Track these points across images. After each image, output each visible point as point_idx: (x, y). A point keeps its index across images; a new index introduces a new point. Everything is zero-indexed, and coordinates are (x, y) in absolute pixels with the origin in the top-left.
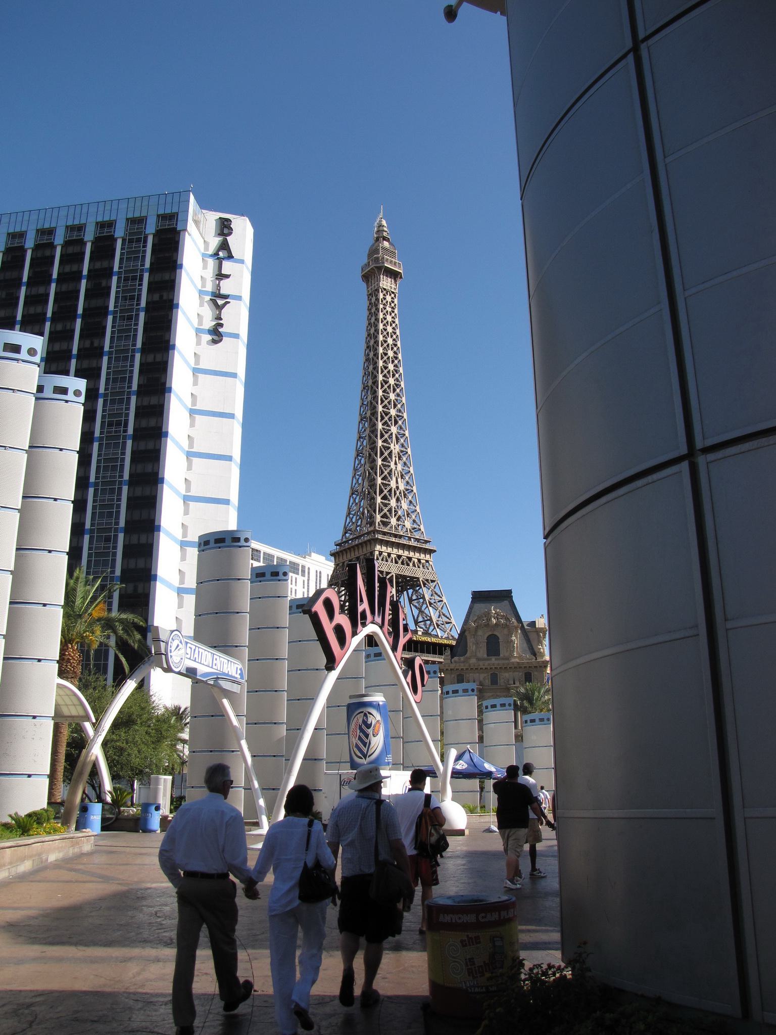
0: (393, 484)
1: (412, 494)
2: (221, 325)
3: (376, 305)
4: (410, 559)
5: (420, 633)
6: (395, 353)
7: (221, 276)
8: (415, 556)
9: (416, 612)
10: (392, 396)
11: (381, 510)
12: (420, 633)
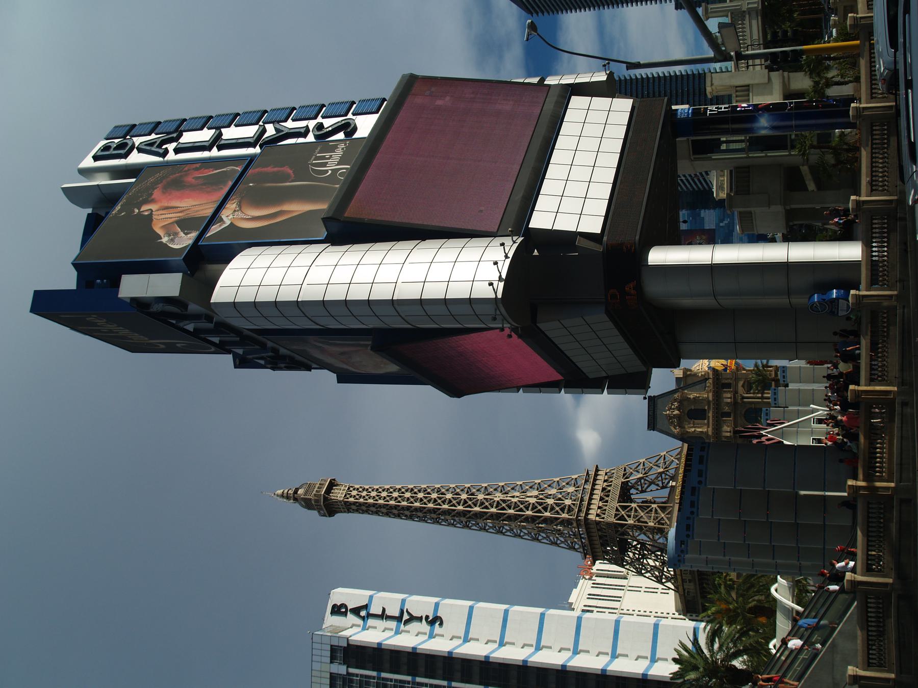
0: (533, 500)
1: (542, 484)
2: (427, 617)
3: (361, 504)
4: (604, 489)
5: (674, 484)
6: (407, 491)
7: (383, 616)
8: (600, 485)
9: (653, 487)
10: (449, 496)
11: (557, 513)
12: (674, 484)
